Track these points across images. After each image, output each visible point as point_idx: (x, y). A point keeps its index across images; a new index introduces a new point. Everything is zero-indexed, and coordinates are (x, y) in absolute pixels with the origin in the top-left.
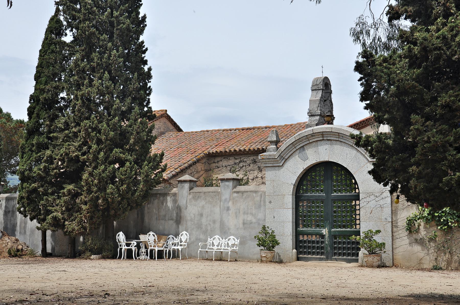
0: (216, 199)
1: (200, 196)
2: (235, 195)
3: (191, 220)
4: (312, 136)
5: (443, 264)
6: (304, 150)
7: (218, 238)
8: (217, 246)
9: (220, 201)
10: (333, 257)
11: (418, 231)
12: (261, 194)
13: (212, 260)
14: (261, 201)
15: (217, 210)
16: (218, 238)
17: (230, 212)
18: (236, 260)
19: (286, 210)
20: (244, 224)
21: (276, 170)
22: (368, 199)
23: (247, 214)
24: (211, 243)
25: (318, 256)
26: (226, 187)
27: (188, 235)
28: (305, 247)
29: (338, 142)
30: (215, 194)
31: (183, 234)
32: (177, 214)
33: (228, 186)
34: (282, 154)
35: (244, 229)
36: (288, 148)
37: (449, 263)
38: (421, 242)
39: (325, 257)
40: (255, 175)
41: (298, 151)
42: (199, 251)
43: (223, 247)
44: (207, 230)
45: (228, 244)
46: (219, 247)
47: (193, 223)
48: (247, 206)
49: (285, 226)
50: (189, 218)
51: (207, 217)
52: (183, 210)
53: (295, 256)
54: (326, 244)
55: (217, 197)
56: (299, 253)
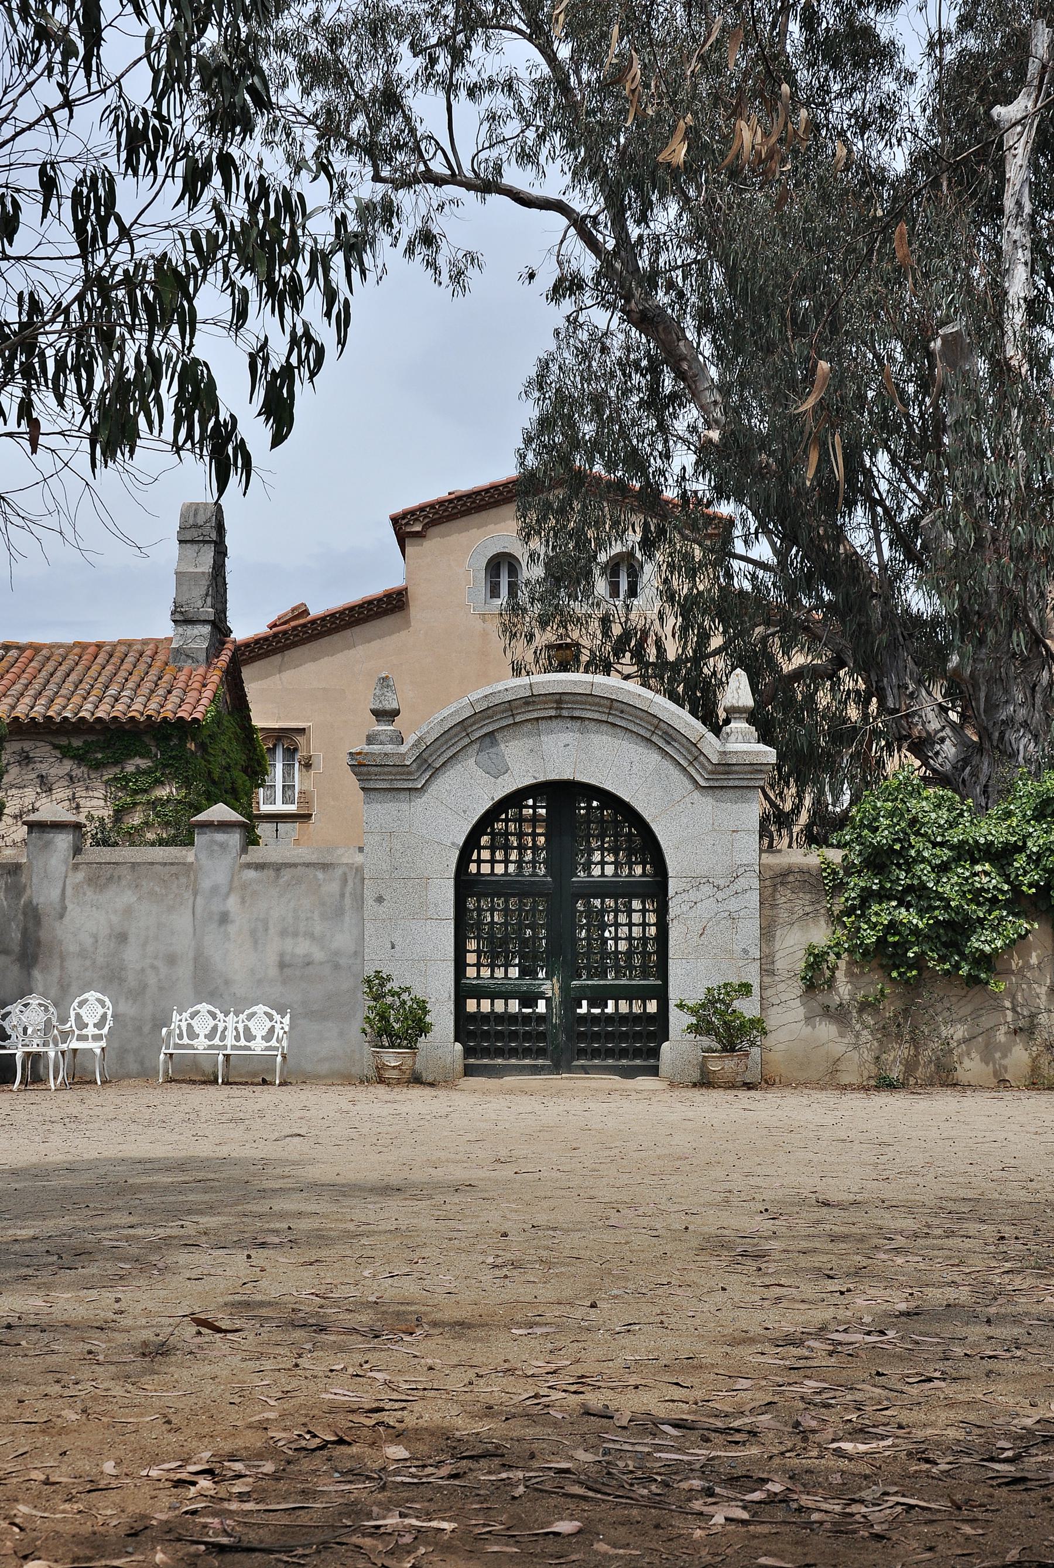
0: (178, 887)
1: (116, 874)
2: (251, 874)
3: (83, 954)
4: (527, 703)
5: (896, 1073)
6: (494, 743)
7: (209, 1012)
8: (263, 1038)
9: (195, 894)
10: (575, 1063)
11: (831, 982)
12: (345, 874)
13: (216, 1082)
14: (342, 895)
15: (182, 921)
16: (209, 1012)
17: (232, 929)
18: (264, 1082)
19: (434, 923)
20: (282, 965)
21: (399, 800)
22: (693, 895)
23: (296, 935)
24: (184, 1029)
25: (527, 1062)
26: (216, 848)
27: (108, 1003)
28: (486, 1036)
29: (604, 728)
30: (174, 869)
31: (87, 1000)
32: (25, 932)
33: (223, 846)
34: (428, 752)
35: (284, 983)
36: (447, 736)
37: (910, 1067)
38: (838, 1015)
39: (548, 1063)
40: (27, 801)
41: (476, 746)
42: (162, 1056)
43: (230, 1041)
44: (144, 987)
45: (247, 1029)
46: (216, 1041)
47: (88, 963)
48: (295, 910)
49: (429, 972)
50: (73, 948)
51: (144, 945)
52: (45, 921)
53: (459, 1067)
54: (555, 1026)
55: (183, 880)
56: (468, 1052)
